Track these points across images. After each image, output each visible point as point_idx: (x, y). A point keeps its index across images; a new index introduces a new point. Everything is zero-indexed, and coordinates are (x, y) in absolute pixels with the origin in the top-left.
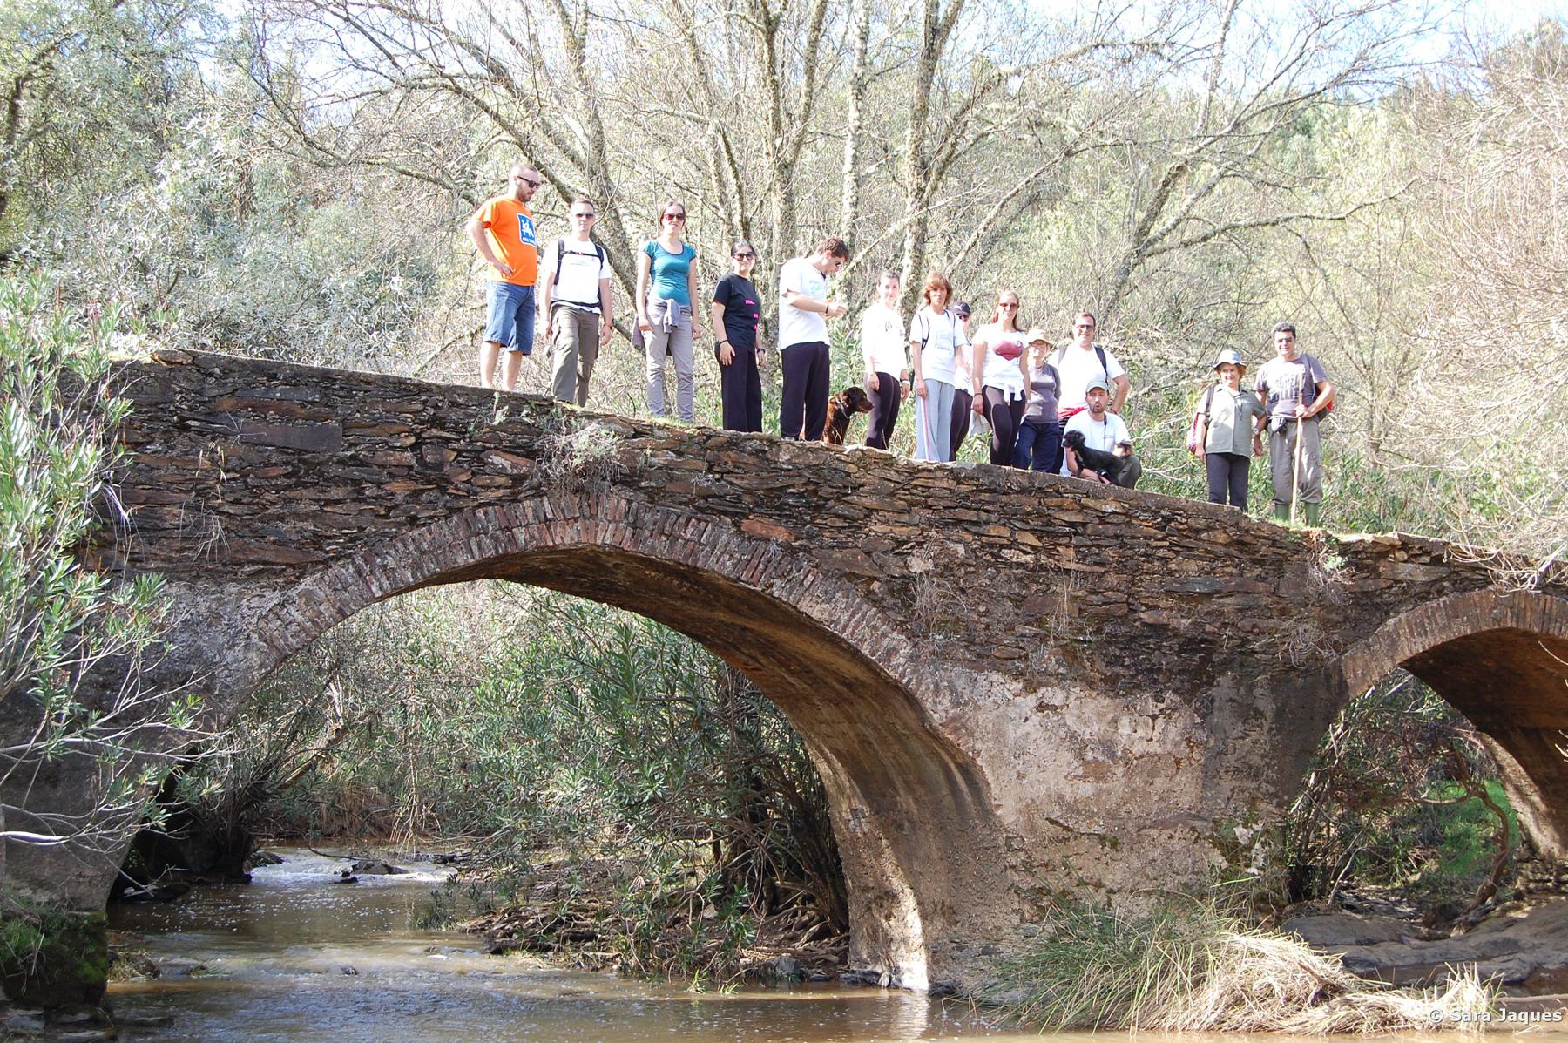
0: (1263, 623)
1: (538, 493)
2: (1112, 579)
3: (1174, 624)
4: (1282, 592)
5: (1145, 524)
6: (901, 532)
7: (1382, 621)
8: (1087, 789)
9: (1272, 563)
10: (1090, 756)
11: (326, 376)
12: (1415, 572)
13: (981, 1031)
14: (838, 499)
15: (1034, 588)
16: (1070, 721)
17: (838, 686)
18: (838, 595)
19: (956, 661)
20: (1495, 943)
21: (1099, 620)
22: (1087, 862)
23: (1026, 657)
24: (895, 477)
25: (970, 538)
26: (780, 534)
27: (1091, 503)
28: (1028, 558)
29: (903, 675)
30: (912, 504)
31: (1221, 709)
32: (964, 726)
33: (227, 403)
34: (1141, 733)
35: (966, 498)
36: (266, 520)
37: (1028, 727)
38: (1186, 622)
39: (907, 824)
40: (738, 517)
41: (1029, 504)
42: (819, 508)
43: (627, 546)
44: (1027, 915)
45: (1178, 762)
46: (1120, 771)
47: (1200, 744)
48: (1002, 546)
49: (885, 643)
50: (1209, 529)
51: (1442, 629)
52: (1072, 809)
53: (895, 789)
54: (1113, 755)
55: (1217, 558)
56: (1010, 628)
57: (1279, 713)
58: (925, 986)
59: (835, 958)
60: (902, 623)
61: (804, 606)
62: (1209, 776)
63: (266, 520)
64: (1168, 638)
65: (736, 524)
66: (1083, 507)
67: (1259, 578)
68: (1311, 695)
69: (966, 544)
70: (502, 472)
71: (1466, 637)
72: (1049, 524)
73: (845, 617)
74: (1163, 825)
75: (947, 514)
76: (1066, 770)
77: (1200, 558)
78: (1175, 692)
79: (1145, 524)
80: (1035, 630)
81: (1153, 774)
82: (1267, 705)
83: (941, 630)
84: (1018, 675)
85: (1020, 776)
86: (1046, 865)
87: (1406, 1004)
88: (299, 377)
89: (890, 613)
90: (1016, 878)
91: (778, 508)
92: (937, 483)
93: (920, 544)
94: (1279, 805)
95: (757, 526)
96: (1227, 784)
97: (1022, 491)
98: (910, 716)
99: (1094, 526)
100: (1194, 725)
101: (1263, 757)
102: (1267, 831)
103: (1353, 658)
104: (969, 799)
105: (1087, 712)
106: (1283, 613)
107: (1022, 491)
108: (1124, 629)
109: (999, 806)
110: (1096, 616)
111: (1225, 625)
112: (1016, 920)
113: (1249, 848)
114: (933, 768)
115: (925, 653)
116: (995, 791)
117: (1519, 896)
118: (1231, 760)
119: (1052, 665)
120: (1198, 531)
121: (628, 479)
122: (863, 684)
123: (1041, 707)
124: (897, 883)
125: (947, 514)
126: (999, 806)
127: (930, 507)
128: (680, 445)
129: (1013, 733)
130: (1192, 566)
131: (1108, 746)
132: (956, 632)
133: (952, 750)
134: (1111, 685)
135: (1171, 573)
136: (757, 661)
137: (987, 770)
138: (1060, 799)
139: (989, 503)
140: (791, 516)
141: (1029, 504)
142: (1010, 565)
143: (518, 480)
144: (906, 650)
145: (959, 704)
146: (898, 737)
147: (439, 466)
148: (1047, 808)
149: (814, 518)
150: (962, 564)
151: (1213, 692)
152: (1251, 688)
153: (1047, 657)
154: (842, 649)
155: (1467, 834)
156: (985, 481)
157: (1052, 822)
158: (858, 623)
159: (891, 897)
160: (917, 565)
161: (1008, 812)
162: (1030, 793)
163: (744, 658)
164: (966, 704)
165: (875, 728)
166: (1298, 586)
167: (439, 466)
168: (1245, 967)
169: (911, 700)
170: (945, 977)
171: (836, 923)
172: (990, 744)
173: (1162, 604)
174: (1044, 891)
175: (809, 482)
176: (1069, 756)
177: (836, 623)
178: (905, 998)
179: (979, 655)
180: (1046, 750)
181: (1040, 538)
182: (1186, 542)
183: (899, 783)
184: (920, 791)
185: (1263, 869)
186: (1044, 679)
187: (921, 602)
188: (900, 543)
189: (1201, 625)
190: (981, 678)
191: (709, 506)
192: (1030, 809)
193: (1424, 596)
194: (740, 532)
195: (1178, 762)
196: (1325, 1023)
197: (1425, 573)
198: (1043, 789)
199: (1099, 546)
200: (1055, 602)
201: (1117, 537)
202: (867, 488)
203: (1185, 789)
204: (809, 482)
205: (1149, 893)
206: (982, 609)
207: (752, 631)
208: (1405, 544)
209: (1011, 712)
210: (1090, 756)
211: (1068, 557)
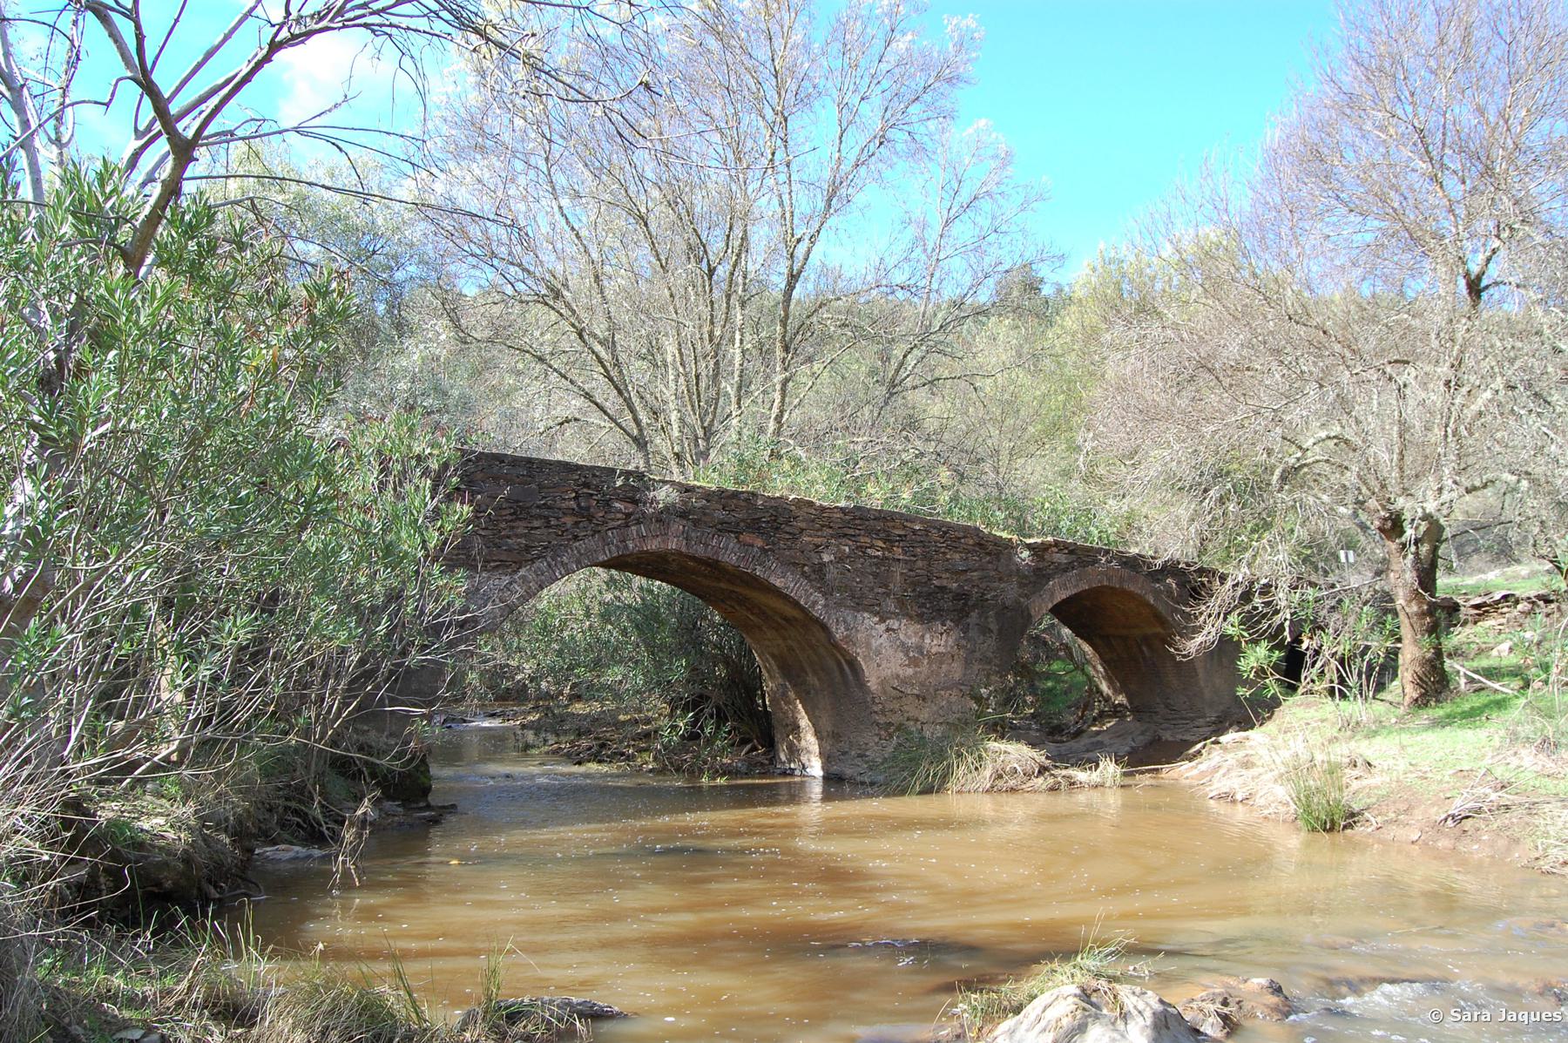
1: (638, 522)
2: (920, 564)
6: (818, 541)
8: (910, 671)
11: (530, 461)
12: (1061, 558)
19: (847, 607)
21: (914, 584)
26: (759, 543)
33: (479, 476)
36: (501, 538)
43: (684, 550)
47: (964, 647)
52: (904, 681)
56: (872, 589)
57: (1000, 631)
58: (821, 773)
61: (772, 580)
62: (967, 663)
63: (501, 538)
68: (1014, 622)
70: (620, 511)
74: (947, 689)
82: (994, 627)
84: (876, 614)
87: (1081, 775)
88: (516, 462)
98: (822, 636)
99: (911, 536)
105: (909, 632)
114: (831, 663)
117: (1095, 719)
121: (683, 515)
123: (888, 630)
124: (804, 722)
128: (708, 495)
129: (875, 643)
130: (957, 556)
131: (920, 649)
133: (844, 653)
134: (920, 619)
143: (628, 515)
147: (588, 508)
153: (890, 605)
155: (1054, 688)
160: (826, 558)
161: (873, 684)
162: (883, 674)
167: (588, 508)
169: (824, 628)
170: (835, 769)
171: (770, 745)
174: (890, 724)
180: (891, 651)
191: (724, 528)
192: (883, 682)
193: (1065, 571)
203: (956, 670)
208: (1056, 544)
211: (898, 552)
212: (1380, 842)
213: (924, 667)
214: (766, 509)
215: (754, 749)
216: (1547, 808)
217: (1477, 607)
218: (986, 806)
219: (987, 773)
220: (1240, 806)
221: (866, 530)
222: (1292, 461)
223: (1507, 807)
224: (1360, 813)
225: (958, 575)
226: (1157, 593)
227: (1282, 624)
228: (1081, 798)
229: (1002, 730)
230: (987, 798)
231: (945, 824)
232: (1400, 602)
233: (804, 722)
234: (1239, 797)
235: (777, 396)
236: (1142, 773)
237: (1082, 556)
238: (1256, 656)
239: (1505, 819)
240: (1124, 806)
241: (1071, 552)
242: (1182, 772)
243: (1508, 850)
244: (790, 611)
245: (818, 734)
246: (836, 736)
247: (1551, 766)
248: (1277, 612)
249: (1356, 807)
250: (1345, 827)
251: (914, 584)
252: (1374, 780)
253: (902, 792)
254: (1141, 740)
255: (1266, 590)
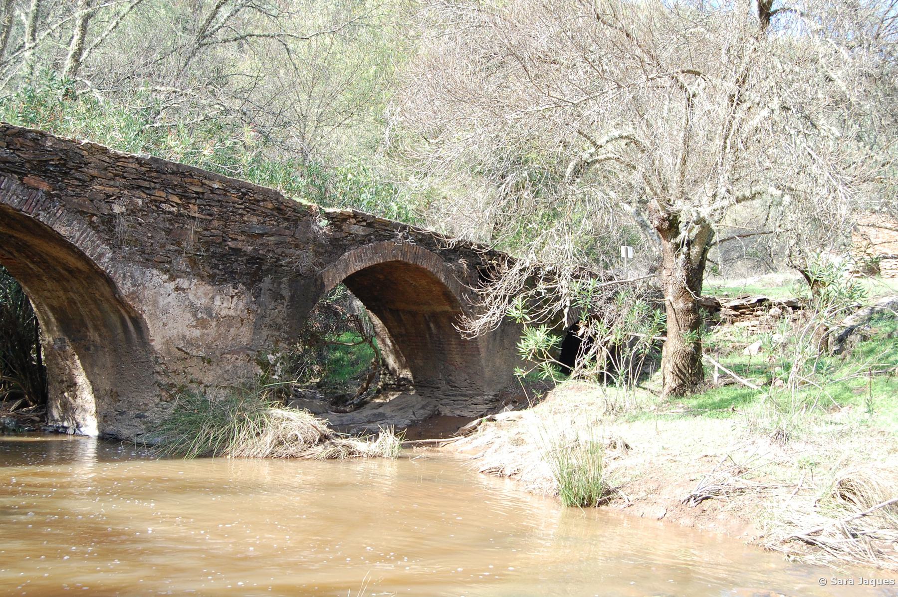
0: (288, 251)
2: (216, 223)
3: (244, 249)
4: (297, 236)
5: (233, 195)
6: (109, 190)
7: (343, 253)
8: (197, 333)
9: (293, 221)
10: (200, 315)
12: (359, 230)
13: (147, 458)
14: (76, 170)
15: (177, 225)
16: (191, 297)
17: (62, 271)
18: (75, 222)
20: (375, 415)
21: (209, 244)
22: (196, 372)
23: (170, 262)
24: (108, 160)
25: (144, 196)
26: (45, 187)
27: (207, 182)
28: (174, 209)
29: (107, 268)
30: (116, 175)
31: (265, 294)
32: (137, 297)
34: (225, 305)
35: (144, 174)
37: (169, 299)
38: (250, 248)
39: (92, 348)
40: (22, 175)
41: (176, 180)
42: (66, 174)
44: (164, 398)
45: (242, 320)
46: (214, 324)
47: (254, 311)
48: (161, 202)
49: (98, 250)
50: (264, 200)
51: (370, 259)
52: (189, 343)
53: (87, 328)
54: (211, 316)
55: (267, 216)
56: (163, 246)
57: (292, 298)
58: (96, 433)
59: (37, 419)
60: (108, 240)
62: (257, 328)
64: (241, 256)
65: (21, 179)
66: (203, 184)
67: (286, 228)
68: (306, 291)
69: (143, 199)
71: (379, 264)
72: (186, 192)
73: (78, 235)
75: (134, 182)
76: (187, 322)
77: (258, 215)
78: (243, 284)
79: (233, 195)
80: (176, 248)
81: (230, 326)
82: (286, 293)
83: (128, 245)
84: (166, 271)
85: (165, 325)
86: (175, 372)
87: (359, 445)
89: (102, 234)
90: (159, 378)
91: (44, 172)
92: (130, 165)
93: (119, 198)
94: (289, 344)
95: (32, 181)
96: (265, 332)
97: (173, 173)
98: (106, 290)
100: (251, 302)
101: (283, 319)
102: (283, 357)
103: (328, 271)
104: (134, 335)
105: (199, 292)
106: (297, 246)
107: (173, 173)
108: (220, 250)
109: (153, 340)
110: (206, 242)
111: (269, 251)
112: (157, 400)
113: (274, 365)
114: (114, 319)
115: (119, 257)
116: (151, 332)
117: (379, 392)
118: (268, 320)
119: (184, 267)
120: (258, 201)
122: (80, 271)
123: (177, 289)
124: (81, 379)
125: (134, 182)
126: (153, 340)
127: (125, 178)
129: (162, 302)
130: (255, 219)
131: (209, 310)
132: (136, 246)
134: (212, 279)
135: (244, 222)
136: (11, 253)
137: (148, 321)
138: (184, 337)
139: (156, 178)
140: (51, 177)
141: (176, 180)
142: (164, 212)
144: (109, 255)
145: (135, 285)
146: (95, 301)
148: (177, 342)
149: (63, 179)
150: (140, 210)
151: (261, 285)
152: (280, 284)
153: (182, 263)
154: (74, 252)
155: (342, 359)
156: (154, 166)
157: (179, 349)
158: (85, 238)
159: (72, 385)
160: (117, 209)
161: (157, 344)
163: (4, 252)
164: (139, 285)
165: (82, 296)
166: (304, 233)
168: (283, 425)
169: (110, 282)
170: (111, 429)
172: (150, 307)
173: (239, 238)
174: (173, 385)
175: (61, 159)
176: (189, 315)
177: (73, 238)
178: (82, 440)
179: (147, 260)
180: (178, 311)
181: (181, 199)
182: (252, 207)
183: (90, 325)
184: (104, 330)
185: (280, 376)
186: (179, 274)
187: (118, 229)
188: (109, 196)
189: (258, 250)
190: (147, 272)
192: (168, 342)
193: (362, 243)
194: (23, 184)
195: (242, 320)
196: (323, 455)
197: (363, 231)
198: (175, 332)
199: (210, 206)
200: (186, 234)
201: (219, 201)
202: (93, 165)
203: (245, 334)
204: (61, 159)
205: (225, 387)
206: (149, 235)
207: (16, 238)
208: (355, 215)
209: (162, 291)
210: (200, 315)
212: (630, 518)
213: (212, 330)
214: (54, 152)
215: (25, 404)
216: (775, 492)
217: (735, 308)
218: (264, 471)
219: (268, 438)
220: (507, 480)
221: (162, 183)
222: (586, 156)
223: (742, 491)
224: (614, 491)
225: (251, 238)
226: (448, 272)
227: (561, 311)
228: (359, 467)
229: (285, 396)
230: (266, 463)
231: (220, 488)
232: (669, 297)
233: (81, 379)
234: (508, 472)
235: (77, 32)
236: (420, 445)
237: (379, 230)
238: (536, 339)
239: (738, 501)
240: (400, 476)
241: (369, 225)
242: (456, 447)
243: (740, 530)
244: (72, 261)
245: (95, 391)
246: (115, 395)
247: (782, 456)
248: (558, 299)
249: (612, 485)
250: (600, 503)
251: (209, 244)
252: (629, 461)
253: (180, 454)
254: (422, 414)
255: (550, 277)
